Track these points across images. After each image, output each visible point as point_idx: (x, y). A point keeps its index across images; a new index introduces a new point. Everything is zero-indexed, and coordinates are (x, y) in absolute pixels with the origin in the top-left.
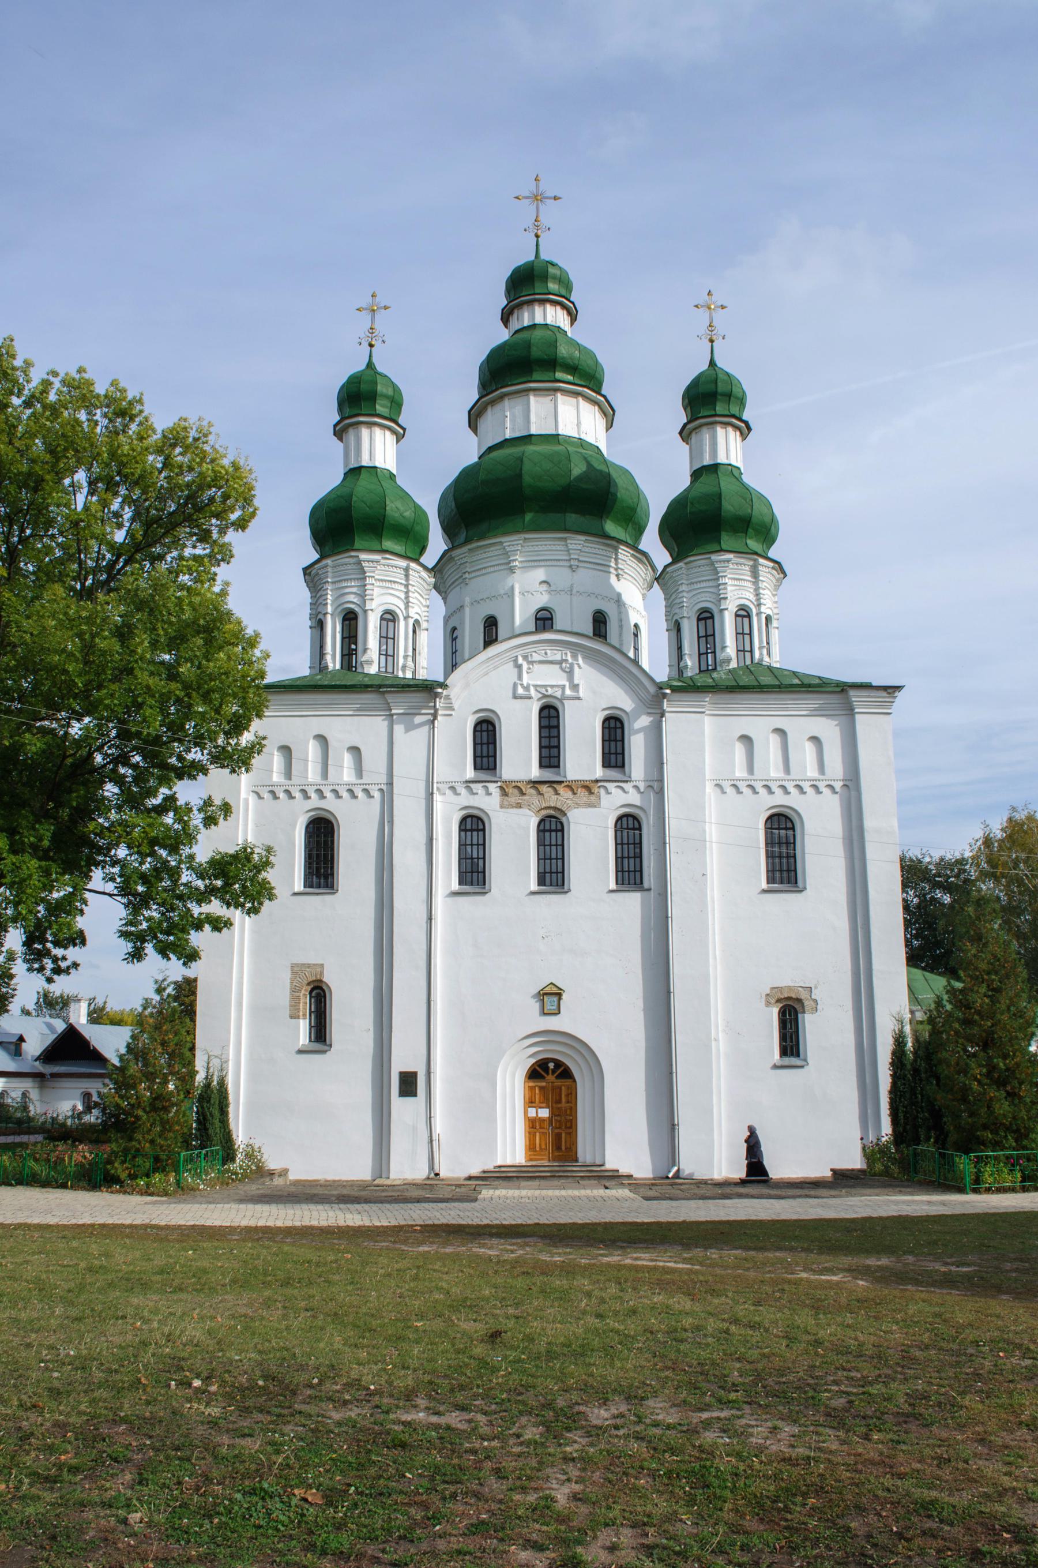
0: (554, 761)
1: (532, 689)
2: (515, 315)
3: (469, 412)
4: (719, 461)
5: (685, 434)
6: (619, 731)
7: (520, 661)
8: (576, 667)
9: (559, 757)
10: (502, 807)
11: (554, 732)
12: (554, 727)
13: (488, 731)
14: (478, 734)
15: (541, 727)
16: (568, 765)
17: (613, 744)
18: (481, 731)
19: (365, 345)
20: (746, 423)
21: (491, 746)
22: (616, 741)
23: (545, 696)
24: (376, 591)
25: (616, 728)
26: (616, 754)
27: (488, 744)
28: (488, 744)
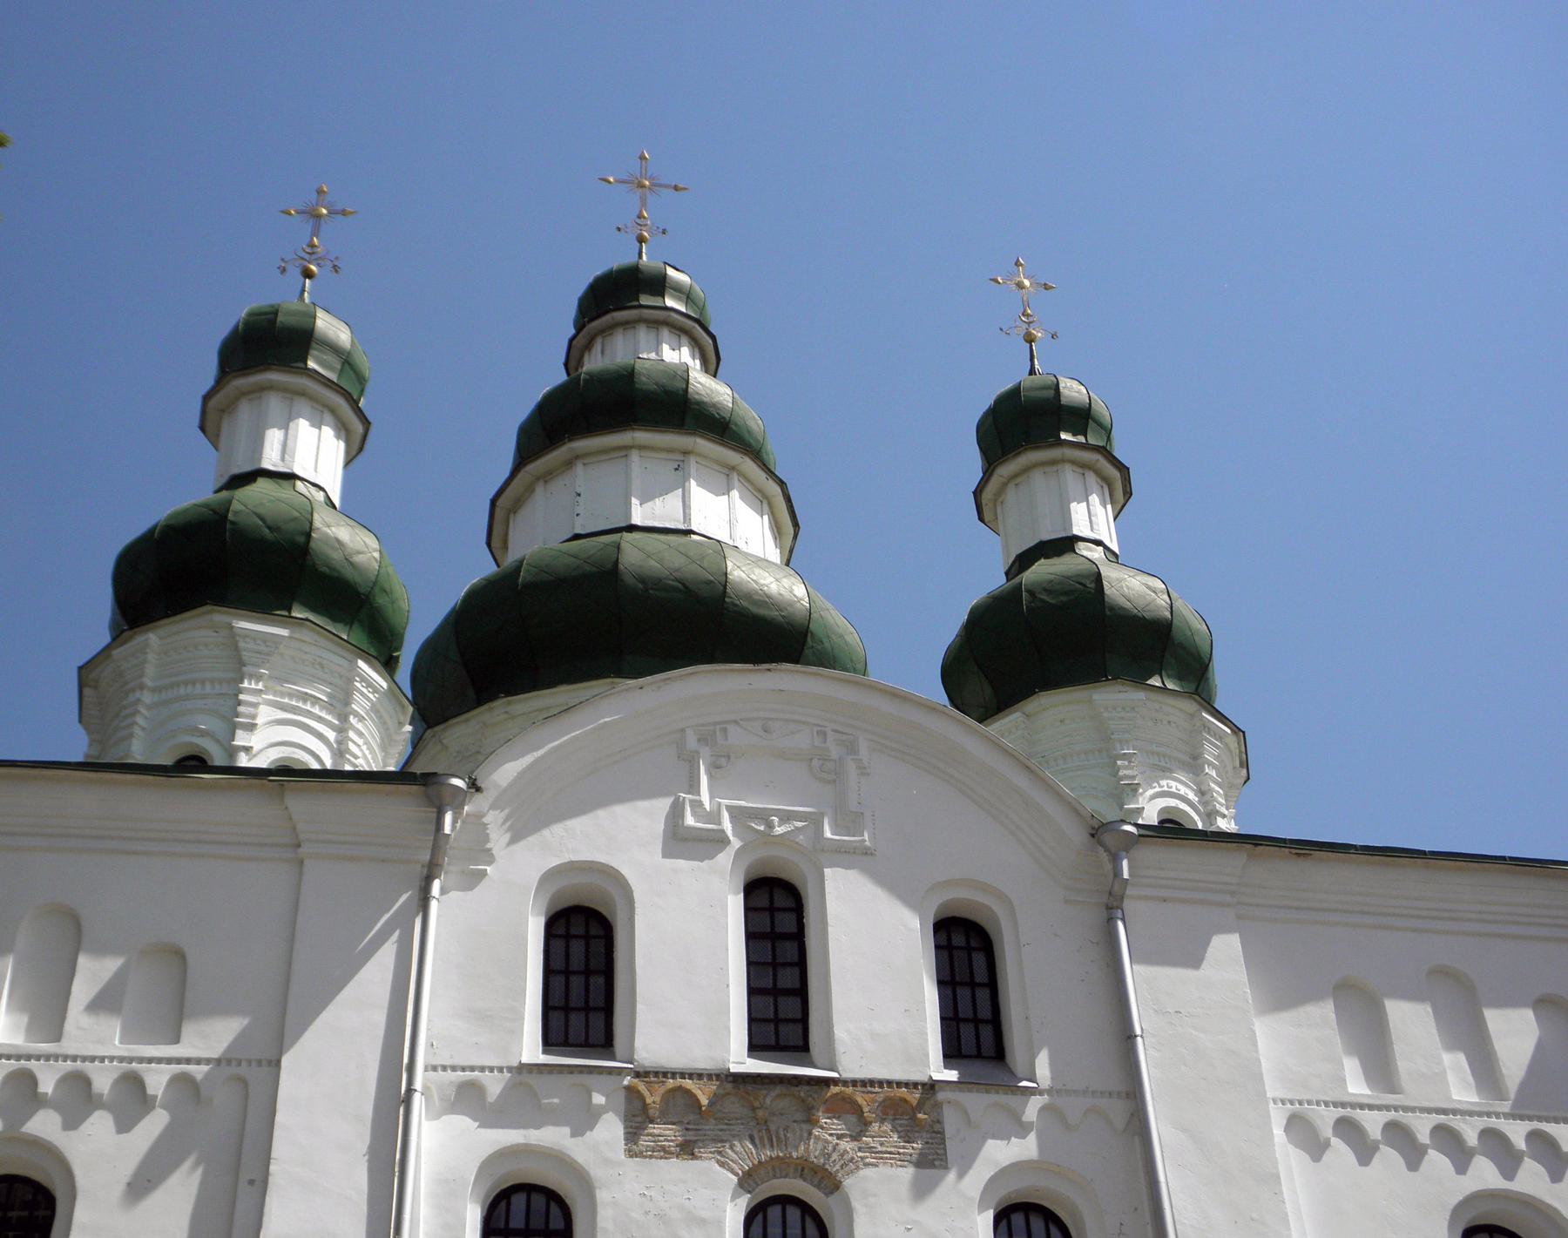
0: (790, 1033)
1: (726, 816)
2: (597, 347)
3: (493, 502)
4: (1076, 531)
5: (983, 504)
6: (979, 959)
7: (691, 741)
8: (851, 768)
9: (804, 1021)
10: (631, 1154)
11: (788, 950)
12: (786, 937)
13: (587, 938)
14: (559, 945)
15: (751, 936)
16: (841, 1032)
17: (964, 994)
18: (567, 937)
19: (296, 273)
20: (1124, 470)
21: (598, 981)
22: (972, 985)
23: (768, 838)
24: (265, 714)
25: (969, 949)
26: (976, 1021)
27: (587, 973)
28: (587, 973)
